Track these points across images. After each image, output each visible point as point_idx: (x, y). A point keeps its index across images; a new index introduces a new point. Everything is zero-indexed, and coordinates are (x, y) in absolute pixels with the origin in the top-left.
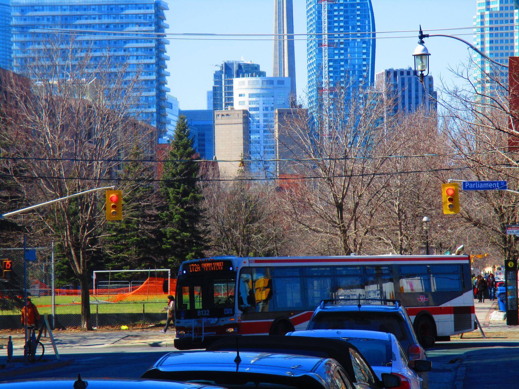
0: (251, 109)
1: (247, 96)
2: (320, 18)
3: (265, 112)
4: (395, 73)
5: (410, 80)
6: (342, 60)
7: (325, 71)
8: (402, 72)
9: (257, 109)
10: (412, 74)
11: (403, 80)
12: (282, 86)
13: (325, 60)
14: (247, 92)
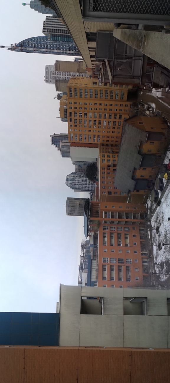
0: (55, 79)
1: (51, 80)
2: (39, 51)
3: (56, 74)
4: (43, 29)
5: (46, 24)
6: (51, 46)
7: (52, 51)
8: (44, 26)
9: (55, 77)
10: (44, 23)
11: (46, 26)
12: (48, 68)
13: (50, 50)
14: (50, 80)
